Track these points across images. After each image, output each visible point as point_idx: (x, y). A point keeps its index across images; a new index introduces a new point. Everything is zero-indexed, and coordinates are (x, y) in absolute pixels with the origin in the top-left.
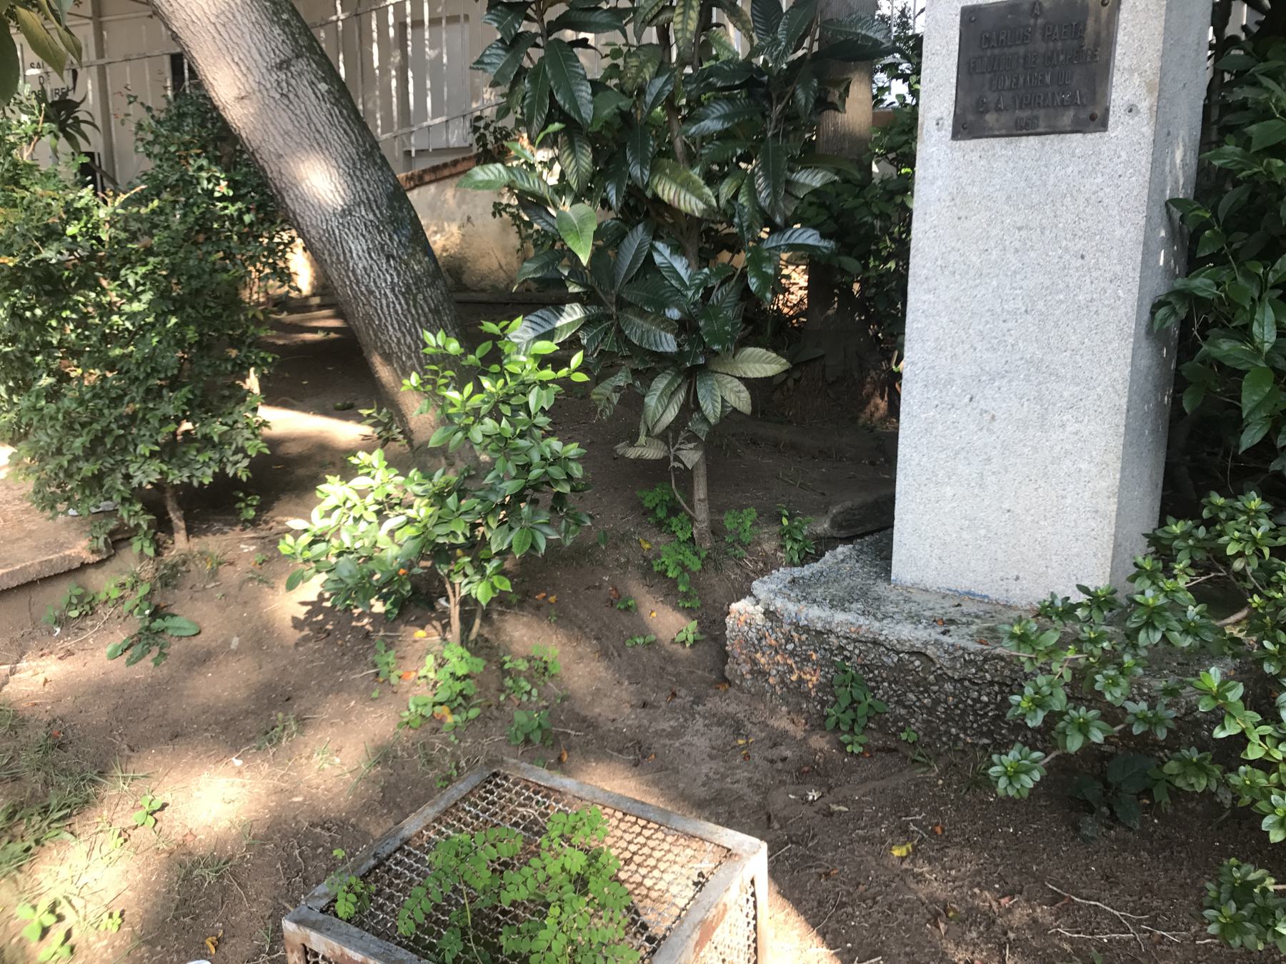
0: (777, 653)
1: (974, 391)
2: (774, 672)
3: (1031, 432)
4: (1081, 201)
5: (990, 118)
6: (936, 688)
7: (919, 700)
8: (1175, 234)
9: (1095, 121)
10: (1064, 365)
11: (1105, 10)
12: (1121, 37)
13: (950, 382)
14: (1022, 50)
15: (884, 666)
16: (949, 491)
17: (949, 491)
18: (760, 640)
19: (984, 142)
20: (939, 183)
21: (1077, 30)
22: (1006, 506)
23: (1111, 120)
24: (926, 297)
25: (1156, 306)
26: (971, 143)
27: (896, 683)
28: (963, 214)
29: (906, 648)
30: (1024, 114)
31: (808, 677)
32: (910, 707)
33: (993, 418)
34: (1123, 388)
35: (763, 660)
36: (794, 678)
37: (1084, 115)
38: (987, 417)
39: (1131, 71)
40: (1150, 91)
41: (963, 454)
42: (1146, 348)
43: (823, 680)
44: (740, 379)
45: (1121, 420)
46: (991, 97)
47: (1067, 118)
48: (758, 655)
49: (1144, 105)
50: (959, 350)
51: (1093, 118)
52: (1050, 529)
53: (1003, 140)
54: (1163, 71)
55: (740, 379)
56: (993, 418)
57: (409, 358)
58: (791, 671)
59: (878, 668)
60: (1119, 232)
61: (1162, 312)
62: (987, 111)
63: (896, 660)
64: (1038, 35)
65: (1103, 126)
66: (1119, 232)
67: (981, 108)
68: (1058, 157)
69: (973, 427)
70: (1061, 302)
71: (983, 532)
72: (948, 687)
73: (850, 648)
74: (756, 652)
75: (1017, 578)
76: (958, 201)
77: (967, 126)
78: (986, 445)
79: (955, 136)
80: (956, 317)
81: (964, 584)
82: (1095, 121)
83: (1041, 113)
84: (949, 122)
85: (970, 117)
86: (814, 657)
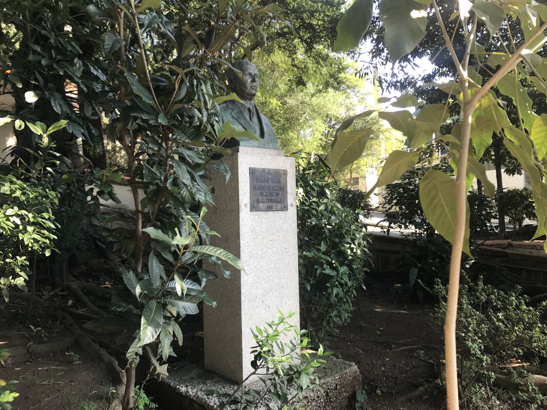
5: (261, 205)
9: (285, 208)
10: (285, 283)
12: (288, 185)
14: (267, 184)
19: (259, 213)
21: (279, 181)
26: (256, 213)
28: (255, 237)
30: (269, 204)
33: (269, 307)
38: (267, 307)
46: (261, 198)
50: (258, 285)
51: (285, 207)
53: (264, 212)
56: (269, 307)
65: (287, 210)
67: (258, 201)
70: (282, 263)
76: (254, 232)
79: (251, 210)
80: (256, 274)
82: (285, 208)
84: (249, 205)
85: (255, 204)
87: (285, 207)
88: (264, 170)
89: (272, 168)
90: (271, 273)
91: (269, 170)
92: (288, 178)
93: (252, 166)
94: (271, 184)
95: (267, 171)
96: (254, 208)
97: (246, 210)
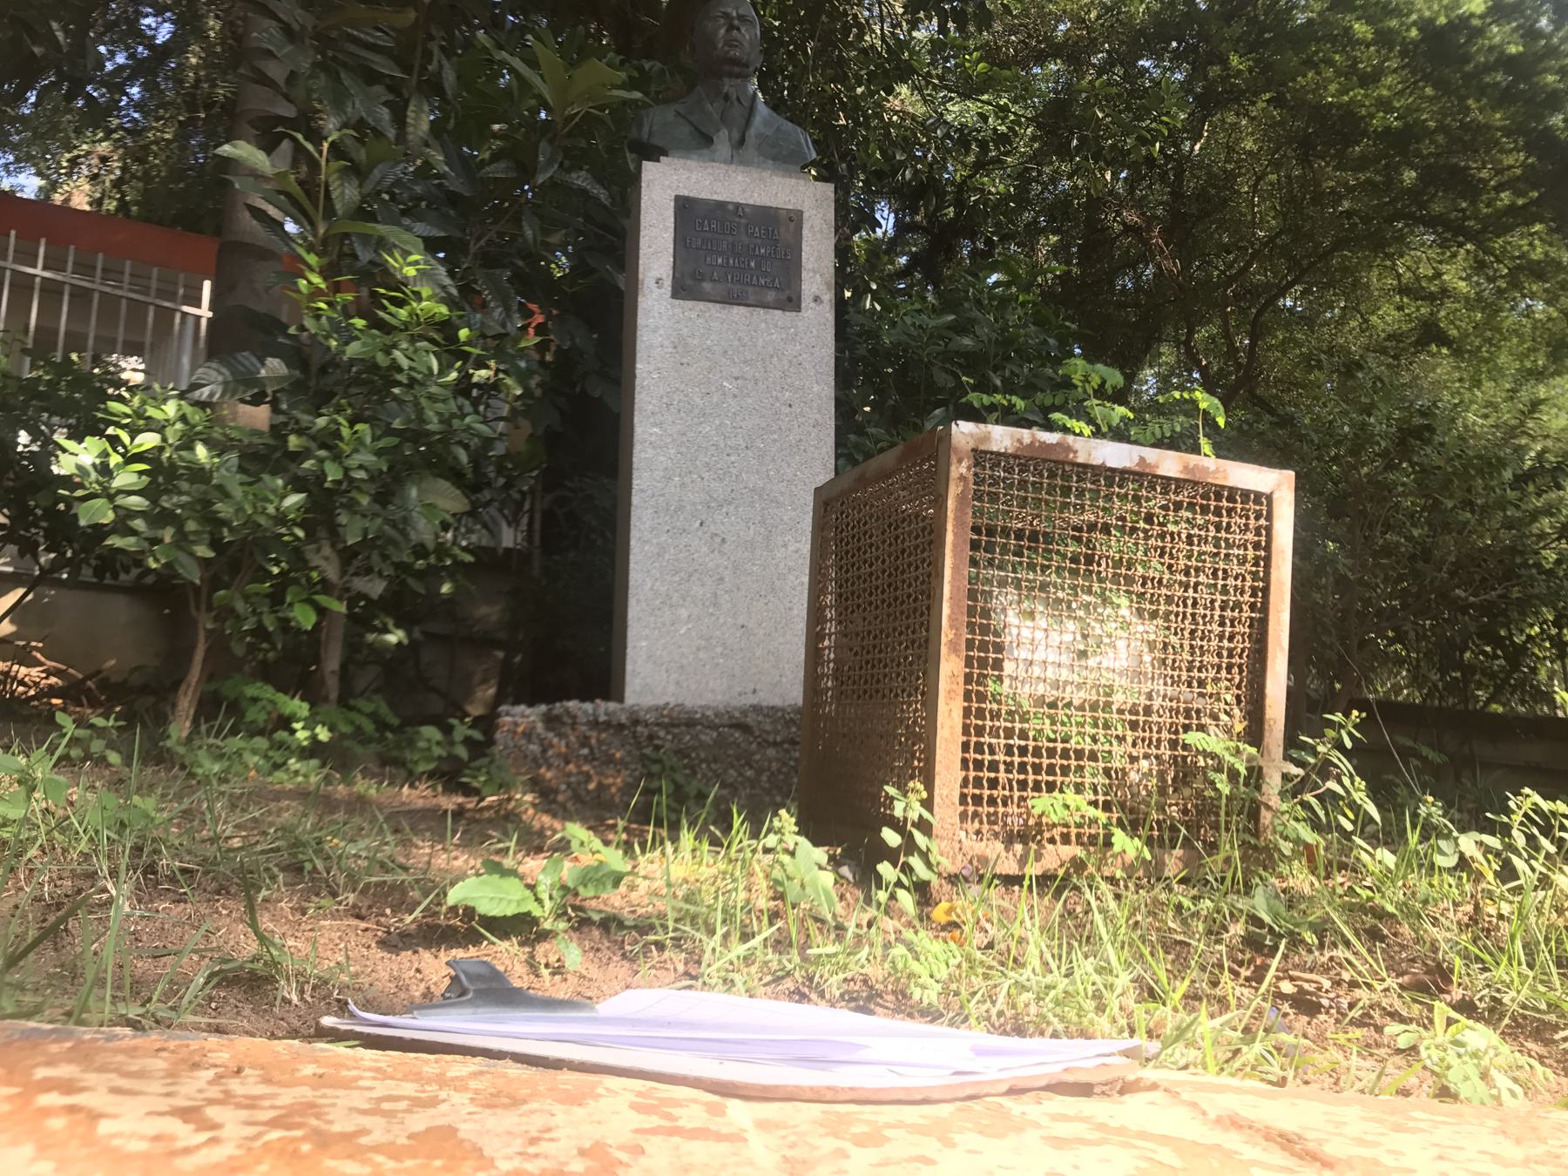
0: (567, 762)
1: (703, 517)
2: (563, 787)
3: (758, 552)
4: (785, 362)
5: (707, 286)
6: (758, 757)
7: (740, 774)
9: (791, 303)
10: (782, 493)
11: (792, 225)
14: (730, 239)
15: (702, 745)
16: (684, 613)
17: (684, 613)
18: (544, 751)
19: (701, 305)
20: (661, 332)
22: (740, 621)
26: (690, 304)
27: (715, 761)
29: (726, 720)
31: (610, 781)
32: (731, 785)
33: (723, 540)
35: (549, 775)
36: (592, 786)
37: (783, 296)
38: (718, 540)
41: (697, 575)
43: (630, 780)
47: (771, 296)
48: (543, 770)
50: (687, 480)
51: (790, 299)
52: (781, 640)
56: (723, 540)
58: (588, 778)
59: (694, 749)
62: (703, 280)
63: (715, 735)
64: (742, 230)
65: (798, 308)
66: (816, 388)
67: (699, 278)
68: (763, 325)
69: (704, 549)
71: (719, 650)
72: (771, 752)
73: (662, 734)
74: (540, 767)
75: (755, 691)
76: (680, 349)
77: (684, 288)
78: (718, 566)
80: (683, 449)
82: (791, 303)
83: (750, 289)
84: (668, 283)
85: (689, 282)
86: (618, 755)
87: (790, 299)
88: (721, 205)
89: (751, 202)
91: (737, 205)
92: (805, 232)
93: (686, 193)
94: (746, 240)
95: (731, 207)
96: (684, 288)
97: (657, 291)
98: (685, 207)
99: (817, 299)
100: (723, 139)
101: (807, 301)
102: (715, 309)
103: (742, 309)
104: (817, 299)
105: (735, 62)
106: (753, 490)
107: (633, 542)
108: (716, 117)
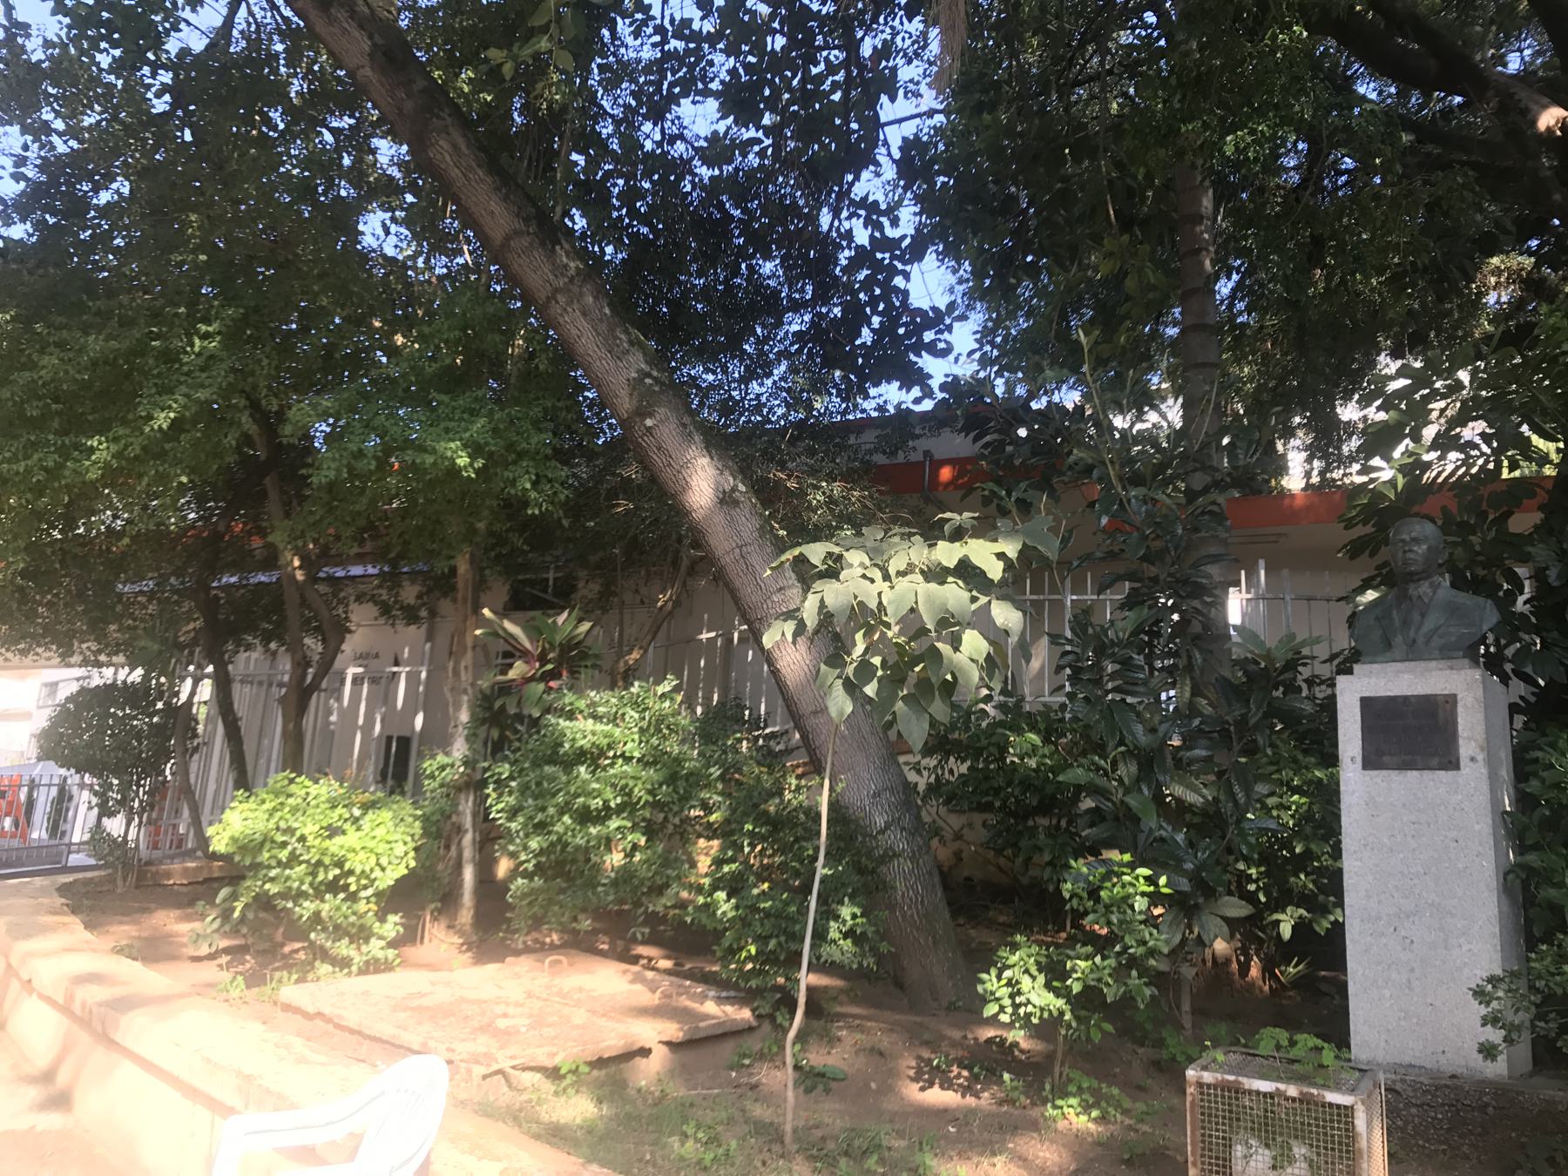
5: (1386, 759)
8: (1510, 835)
9: (1452, 764)
11: (1448, 707)
13: (1379, 918)
16: (1387, 993)
17: (1387, 993)
19: (1384, 772)
23: (1462, 764)
24: (1358, 863)
25: (1506, 874)
34: (1495, 921)
39: (1469, 739)
40: (1482, 749)
42: (1505, 901)
44: (1223, 918)
45: (1497, 941)
47: (1435, 761)
49: (1480, 757)
54: (1487, 739)
55: (1223, 918)
57: (910, 908)
60: (1477, 827)
61: (1511, 877)
66: (1477, 827)
72: (1414, 1110)
79: (1365, 767)
81: (1407, 1059)
82: (1452, 764)
84: (1359, 759)
90: (1416, 881)
92: (1460, 709)
97: (1352, 767)
98: (1367, 703)
99: (1473, 759)
100: (1398, 640)
101: (1464, 761)
102: (1394, 774)
103: (1415, 773)
104: (1473, 759)
105: (1412, 574)
106: (1432, 905)
107: (1348, 942)
108: (1397, 623)
